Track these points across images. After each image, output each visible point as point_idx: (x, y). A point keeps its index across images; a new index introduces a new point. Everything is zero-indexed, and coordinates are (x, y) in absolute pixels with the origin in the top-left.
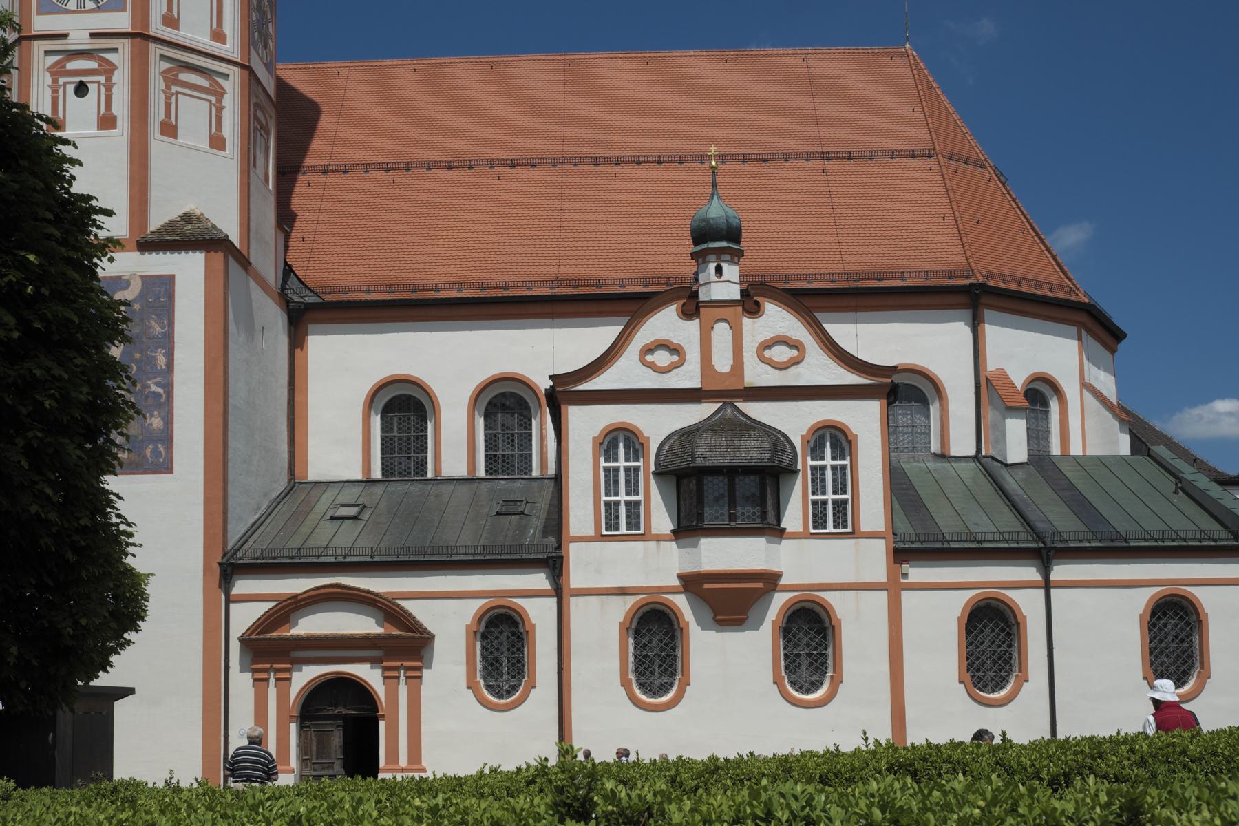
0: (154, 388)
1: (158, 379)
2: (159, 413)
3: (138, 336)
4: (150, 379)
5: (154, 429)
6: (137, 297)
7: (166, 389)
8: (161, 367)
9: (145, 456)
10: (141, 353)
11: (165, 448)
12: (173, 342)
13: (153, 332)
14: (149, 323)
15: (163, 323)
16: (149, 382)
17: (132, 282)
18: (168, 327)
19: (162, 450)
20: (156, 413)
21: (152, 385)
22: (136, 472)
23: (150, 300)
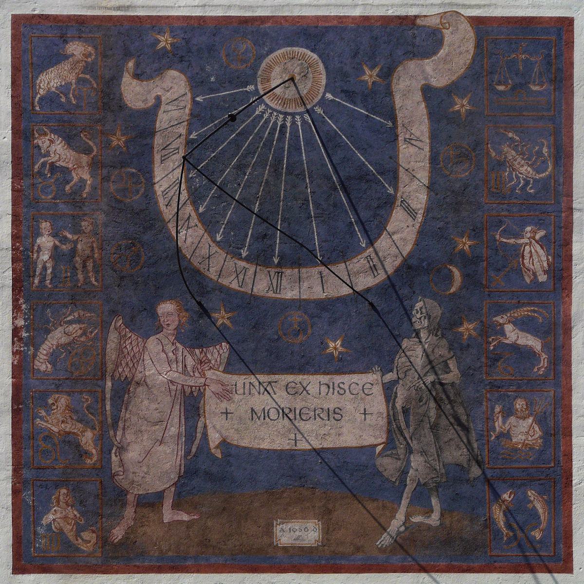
0: (513, 335)
1: (524, 312)
2: (530, 404)
3: (466, 186)
4: (501, 310)
5: (516, 450)
6: (463, 77)
7: (551, 338)
8: (534, 274)
9: (489, 523)
10: (476, 232)
11: (547, 503)
12: (570, 209)
13: (511, 180)
14: (500, 153)
15: (539, 153)
16: (499, 319)
17: (448, 36)
18: (556, 164)
19: (539, 507)
20: (520, 404)
21: (509, 328)
22: (465, 565)
23: (501, 88)
